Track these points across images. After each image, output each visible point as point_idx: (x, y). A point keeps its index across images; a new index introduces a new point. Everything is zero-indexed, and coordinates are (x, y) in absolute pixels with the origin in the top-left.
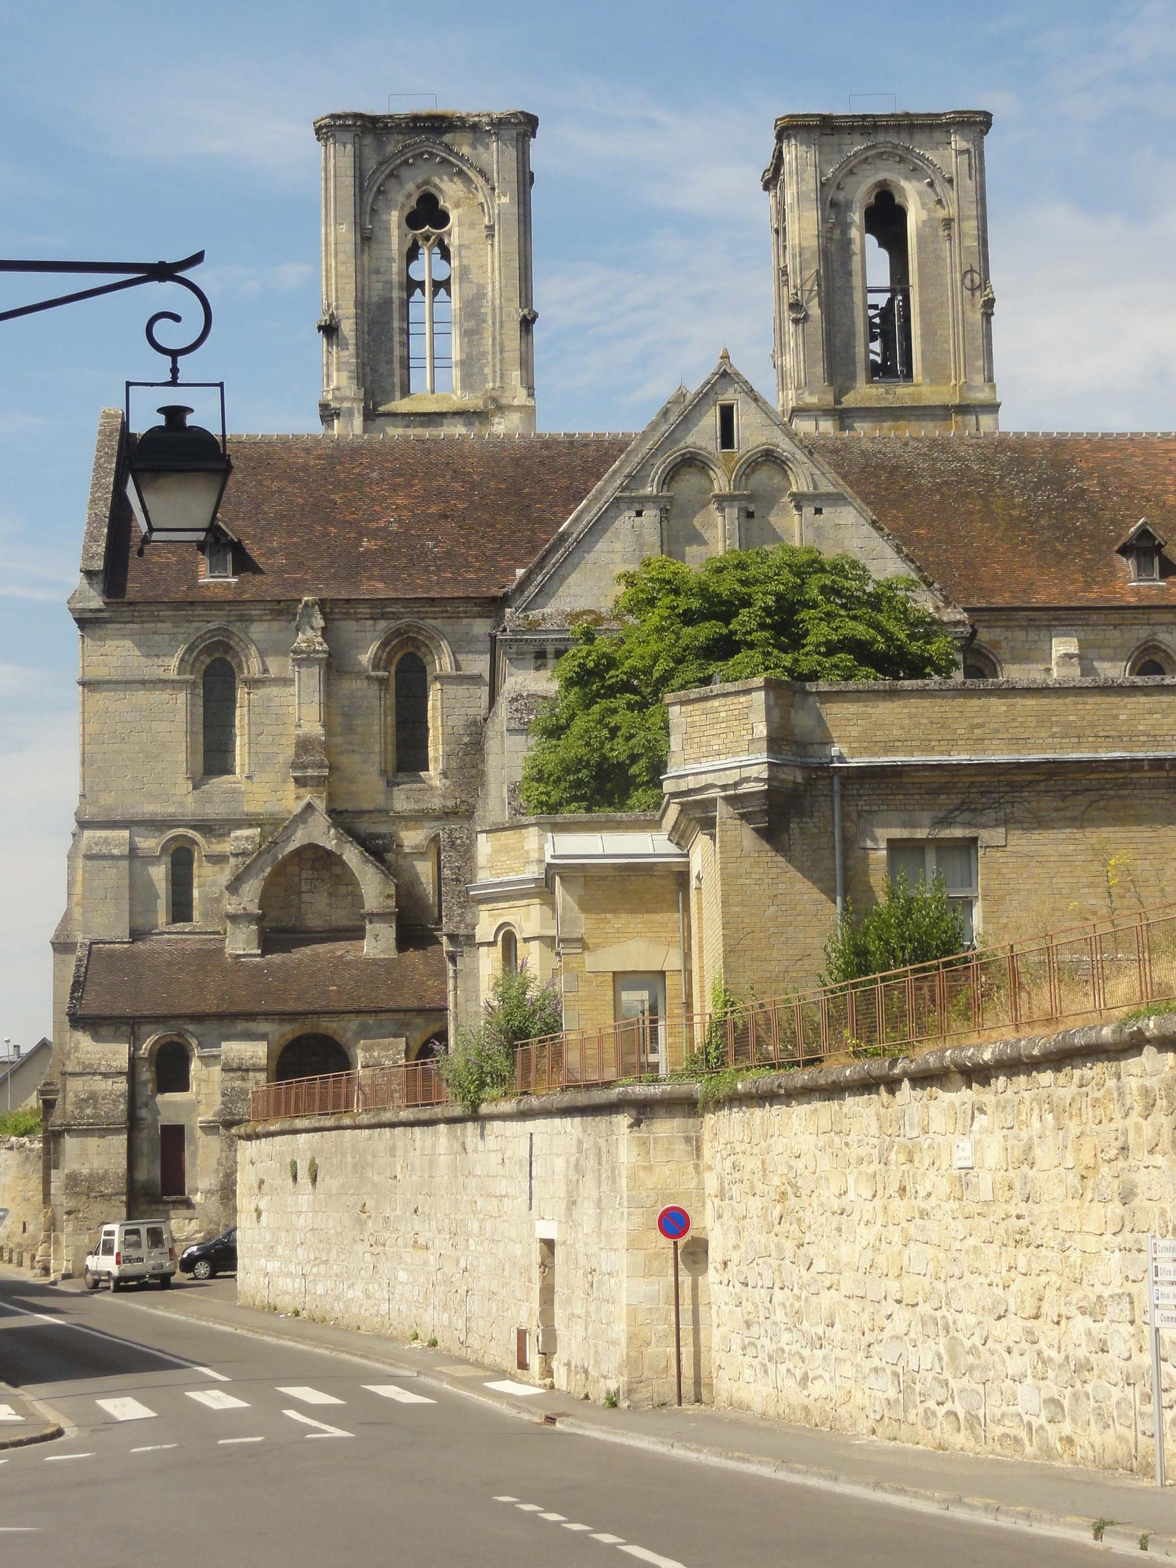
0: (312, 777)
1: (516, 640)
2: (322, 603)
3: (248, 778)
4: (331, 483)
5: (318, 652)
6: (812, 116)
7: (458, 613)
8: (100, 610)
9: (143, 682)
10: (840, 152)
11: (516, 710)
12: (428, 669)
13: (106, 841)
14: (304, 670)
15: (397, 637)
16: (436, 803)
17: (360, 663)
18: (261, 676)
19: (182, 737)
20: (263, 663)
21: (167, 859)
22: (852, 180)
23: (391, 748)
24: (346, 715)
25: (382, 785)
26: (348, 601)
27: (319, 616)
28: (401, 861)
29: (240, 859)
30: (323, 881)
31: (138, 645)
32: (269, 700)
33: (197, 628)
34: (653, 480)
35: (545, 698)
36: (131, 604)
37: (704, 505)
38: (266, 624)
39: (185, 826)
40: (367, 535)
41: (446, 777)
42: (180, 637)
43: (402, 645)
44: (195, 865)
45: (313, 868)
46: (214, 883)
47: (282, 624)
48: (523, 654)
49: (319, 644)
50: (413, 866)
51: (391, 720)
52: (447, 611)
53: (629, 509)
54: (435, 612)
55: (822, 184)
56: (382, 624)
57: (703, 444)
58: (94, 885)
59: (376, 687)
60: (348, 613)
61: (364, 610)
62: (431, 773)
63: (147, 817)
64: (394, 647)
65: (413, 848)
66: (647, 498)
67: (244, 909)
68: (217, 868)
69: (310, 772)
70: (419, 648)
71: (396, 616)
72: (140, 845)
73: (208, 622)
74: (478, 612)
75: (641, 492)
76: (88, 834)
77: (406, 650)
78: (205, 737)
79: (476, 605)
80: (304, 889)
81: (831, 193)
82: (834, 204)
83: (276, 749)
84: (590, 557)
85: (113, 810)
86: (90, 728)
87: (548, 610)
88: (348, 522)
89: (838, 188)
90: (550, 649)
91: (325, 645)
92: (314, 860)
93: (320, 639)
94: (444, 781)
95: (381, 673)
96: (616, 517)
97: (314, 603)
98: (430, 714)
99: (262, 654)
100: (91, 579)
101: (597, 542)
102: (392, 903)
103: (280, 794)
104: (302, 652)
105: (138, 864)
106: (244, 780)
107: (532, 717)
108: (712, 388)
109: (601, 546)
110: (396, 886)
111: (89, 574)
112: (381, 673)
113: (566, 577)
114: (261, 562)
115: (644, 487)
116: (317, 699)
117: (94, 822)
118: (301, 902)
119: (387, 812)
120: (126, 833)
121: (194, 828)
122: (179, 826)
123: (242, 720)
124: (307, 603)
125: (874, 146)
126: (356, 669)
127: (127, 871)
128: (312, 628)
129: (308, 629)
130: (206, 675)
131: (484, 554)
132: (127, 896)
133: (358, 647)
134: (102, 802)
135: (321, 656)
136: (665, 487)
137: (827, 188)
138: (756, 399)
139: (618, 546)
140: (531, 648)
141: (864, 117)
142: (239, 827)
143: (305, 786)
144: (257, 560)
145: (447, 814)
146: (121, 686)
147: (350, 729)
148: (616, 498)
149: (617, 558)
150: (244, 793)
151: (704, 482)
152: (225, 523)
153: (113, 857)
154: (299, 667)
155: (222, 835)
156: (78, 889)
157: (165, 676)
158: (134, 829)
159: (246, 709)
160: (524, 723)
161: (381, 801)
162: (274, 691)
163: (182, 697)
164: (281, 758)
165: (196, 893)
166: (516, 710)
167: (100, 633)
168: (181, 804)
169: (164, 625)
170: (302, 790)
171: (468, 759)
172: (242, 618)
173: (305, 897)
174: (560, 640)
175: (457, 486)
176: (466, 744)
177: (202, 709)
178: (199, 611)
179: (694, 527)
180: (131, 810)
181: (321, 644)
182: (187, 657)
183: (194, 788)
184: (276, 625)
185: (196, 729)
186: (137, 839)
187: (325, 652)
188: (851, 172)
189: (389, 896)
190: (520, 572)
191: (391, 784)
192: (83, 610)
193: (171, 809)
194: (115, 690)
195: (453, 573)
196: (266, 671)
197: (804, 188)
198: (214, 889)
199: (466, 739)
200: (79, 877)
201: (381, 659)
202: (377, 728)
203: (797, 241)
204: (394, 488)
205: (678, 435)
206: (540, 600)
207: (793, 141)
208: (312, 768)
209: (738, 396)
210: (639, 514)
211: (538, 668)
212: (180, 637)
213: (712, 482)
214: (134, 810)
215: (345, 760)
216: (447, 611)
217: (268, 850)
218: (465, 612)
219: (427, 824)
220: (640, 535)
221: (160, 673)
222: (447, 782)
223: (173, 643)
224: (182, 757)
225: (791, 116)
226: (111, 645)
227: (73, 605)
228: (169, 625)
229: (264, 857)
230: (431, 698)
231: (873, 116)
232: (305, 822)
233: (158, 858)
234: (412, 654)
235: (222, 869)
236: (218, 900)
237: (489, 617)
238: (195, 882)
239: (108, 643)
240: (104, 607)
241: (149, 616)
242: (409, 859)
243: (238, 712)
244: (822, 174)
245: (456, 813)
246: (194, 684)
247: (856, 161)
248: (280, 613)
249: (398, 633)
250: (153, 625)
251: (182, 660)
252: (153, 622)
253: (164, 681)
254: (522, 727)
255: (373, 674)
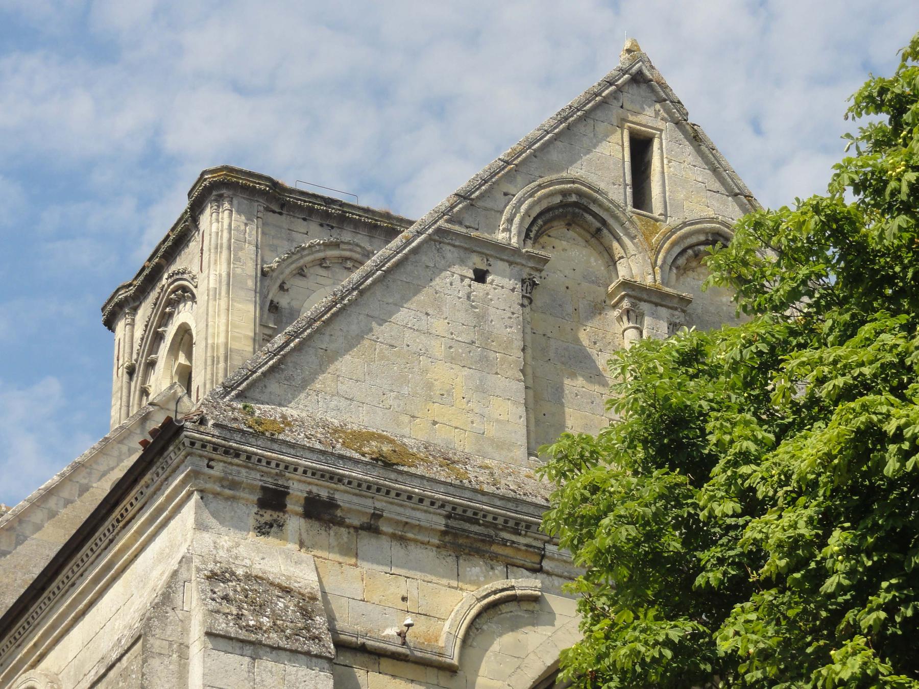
1: (227, 451)
6: (260, 177)
10: (290, 240)
11: (226, 598)
22: (299, 282)
34: (510, 221)
35: (287, 591)
37: (598, 308)
48: (235, 485)
53: (462, 262)
55: (264, 274)
57: (602, 186)
66: (501, 250)
75: (486, 236)
81: (273, 293)
82: (274, 308)
84: (383, 332)
87: (291, 411)
89: (282, 287)
90: (298, 490)
96: (437, 270)
101: (398, 305)
107: (265, 620)
108: (615, 95)
109: (403, 315)
113: (331, 357)
115: (493, 228)
125: (337, 245)
136: (529, 242)
137: (267, 282)
138: (696, 138)
139: (439, 325)
140: (253, 478)
141: (329, 201)
148: (439, 231)
149: (438, 348)
151: (596, 263)
160: (247, 628)
166: (226, 598)
174: (323, 475)
179: (577, 341)
188: (301, 273)
197: (239, 271)
203: (222, 340)
205: (554, 155)
206: (274, 387)
207: (227, 205)
209: (660, 124)
210: (480, 276)
211: (263, 529)
213: (612, 262)
220: (481, 318)
225: (231, 170)
231: (342, 204)
244: (263, 261)
247: (309, 258)
254: (243, 634)
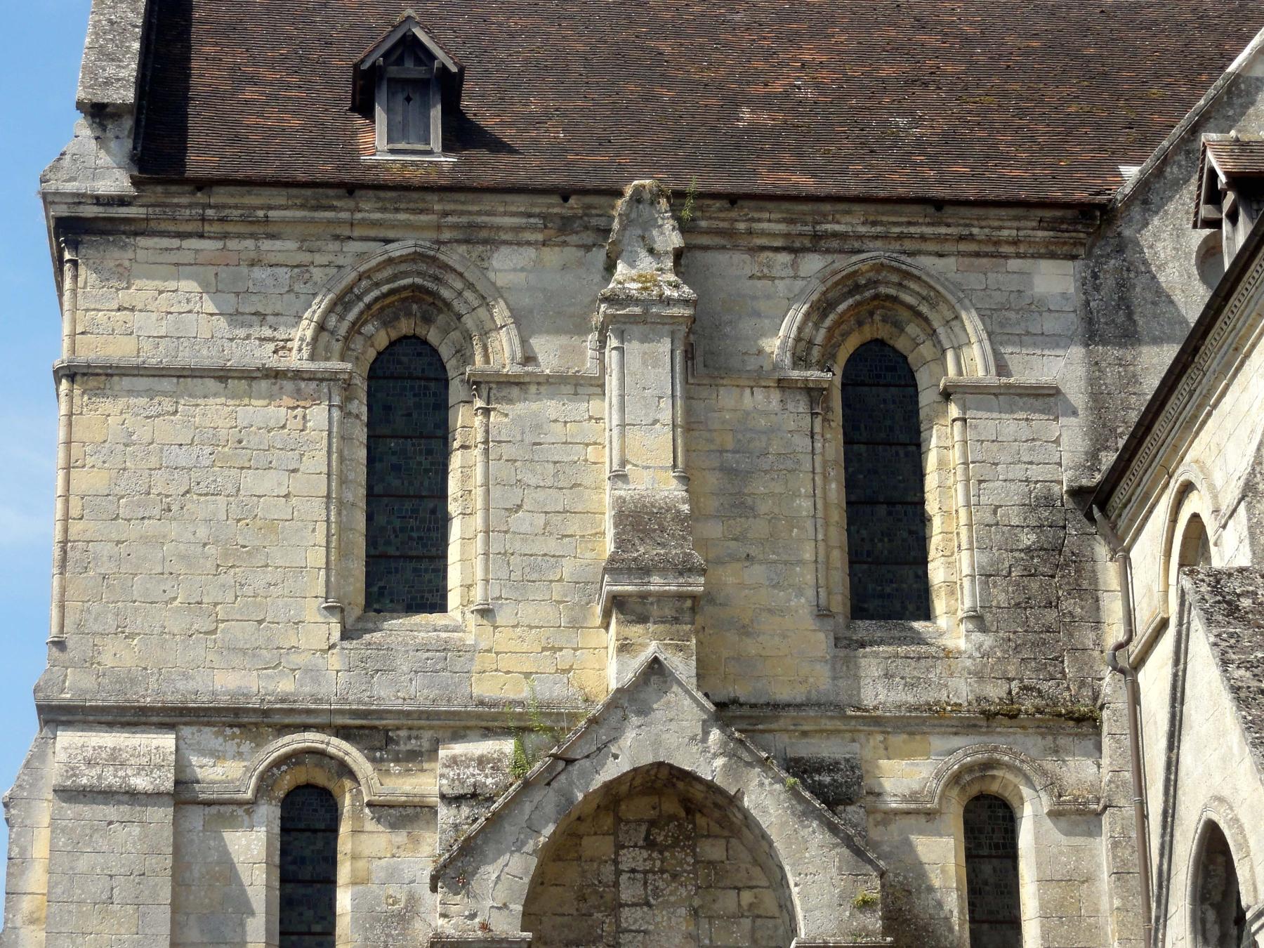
0: (662, 597)
2: (678, 197)
3: (486, 613)
4: (645, 24)
5: (669, 302)
7: (997, 243)
8: (121, 201)
9: (222, 375)
12: (922, 378)
13: (115, 758)
14: (633, 348)
15: (851, 293)
16: (961, 690)
17: (760, 352)
18: (518, 369)
19: (317, 509)
20: (524, 342)
21: (269, 813)
23: (839, 558)
24: (729, 472)
25: (820, 642)
26: (733, 199)
27: (669, 224)
28: (875, 834)
29: (465, 810)
30: (675, 877)
31: (209, 289)
32: (538, 428)
33: (360, 256)
36: (203, 185)
38: (531, 252)
39: (319, 728)
40: (748, 103)
41: (983, 629)
42: (317, 273)
43: (860, 316)
44: (344, 828)
45: (650, 844)
46: (392, 875)
47: (571, 253)
49: (668, 284)
50: (910, 846)
51: (836, 491)
52: (970, 238)
54: (939, 238)
56: (813, 264)
58: (82, 864)
59: (803, 407)
60: (730, 234)
61: (771, 224)
62: (942, 621)
63: (224, 701)
64: (842, 315)
65: (905, 799)
67: (484, 927)
68: (401, 837)
69: (657, 584)
70: (899, 327)
71: (845, 244)
72: (200, 774)
73: (387, 241)
74: (1047, 243)
76: (67, 739)
77: (868, 333)
78: (370, 518)
79: (1042, 224)
80: (625, 896)
83: (552, 546)
85: (133, 681)
86: (83, 481)
88: (699, 83)
91: (686, 289)
92: (653, 823)
93: (672, 277)
94: (978, 637)
95: (814, 374)
97: (660, 193)
98: (931, 481)
99: (524, 323)
100: (104, 129)
102: (874, 922)
103: (564, 658)
104: (630, 300)
105: (196, 818)
106: (472, 620)
110: (882, 875)
111: (98, 113)
112: (814, 374)
114: (507, 135)
116: (666, 416)
117: (83, 710)
118: (620, 931)
119: (839, 707)
120: (166, 741)
121: (345, 733)
122: (306, 728)
123: (465, 478)
124: (638, 191)
126: (752, 364)
127: (168, 832)
128: (651, 251)
129: (643, 253)
130: (374, 374)
131: (1032, 139)
132: (166, 894)
133: (757, 314)
134: (108, 660)
135: (676, 311)
142: (458, 735)
143: (643, 619)
144: (497, 132)
145: (989, 716)
146: (167, 384)
147: (740, 506)
150: (473, 650)
152: (429, 32)
153: (133, 796)
154: (621, 336)
155: (414, 756)
156: (36, 879)
157: (274, 362)
158: (186, 731)
159: (477, 453)
161: (820, 680)
162: (550, 407)
163: (319, 415)
164: (568, 569)
165: (344, 900)
167: (115, 256)
168: (312, 673)
169: (278, 244)
170: (636, 631)
171: (1034, 585)
172: (474, 236)
173: (630, 917)
175: (933, 41)
176: (1028, 550)
177: (362, 454)
178: (369, 209)
180: (181, 685)
181: (677, 287)
182: (332, 321)
183: (345, 636)
184: (552, 256)
185: (349, 496)
186: (194, 760)
187: (686, 302)
189: (866, 905)
190: (1131, 172)
191: (848, 645)
192: (79, 199)
193: (286, 686)
194: (151, 394)
195: (973, 168)
196: (529, 359)
198: (392, 889)
199: (1028, 539)
200: (40, 848)
201: (811, 343)
202: (805, 505)
204: (793, 39)
208: (663, 571)
212: (317, 273)
214: (192, 685)
215: (729, 577)
216: (970, 238)
217: (548, 777)
218: (1015, 242)
219: (937, 743)
221: (264, 356)
222: (988, 641)
223: (299, 287)
224: (317, 557)
226: (142, 290)
227: (52, 186)
228: (291, 245)
229: (538, 795)
230: (934, 442)
232: (644, 711)
233: (253, 803)
234: (880, 343)
235: (416, 841)
236: (405, 916)
237: (1074, 257)
238: (344, 872)
239: (138, 283)
240: (132, 191)
241: (244, 220)
242: (893, 828)
243: (456, 461)
245: (1013, 716)
246: (348, 386)
248: (566, 225)
249: (851, 285)
250: (250, 243)
251: (321, 327)
252: (252, 236)
253: (276, 375)
255: (795, 374)
